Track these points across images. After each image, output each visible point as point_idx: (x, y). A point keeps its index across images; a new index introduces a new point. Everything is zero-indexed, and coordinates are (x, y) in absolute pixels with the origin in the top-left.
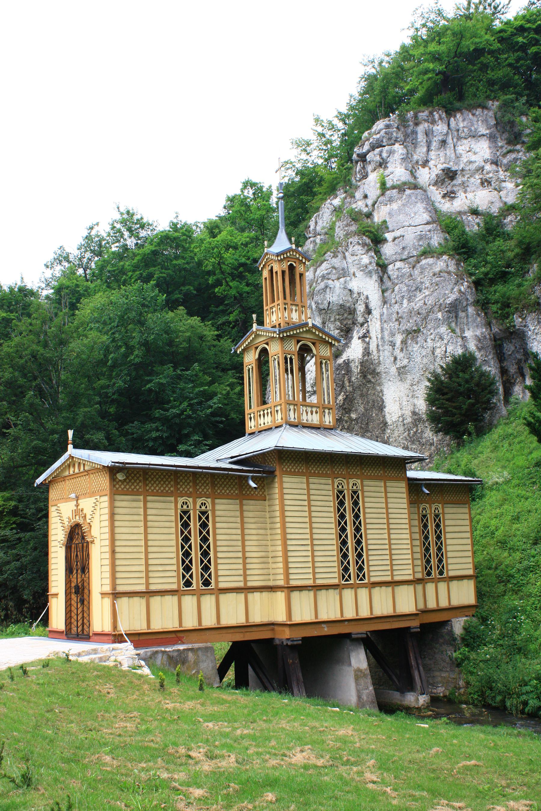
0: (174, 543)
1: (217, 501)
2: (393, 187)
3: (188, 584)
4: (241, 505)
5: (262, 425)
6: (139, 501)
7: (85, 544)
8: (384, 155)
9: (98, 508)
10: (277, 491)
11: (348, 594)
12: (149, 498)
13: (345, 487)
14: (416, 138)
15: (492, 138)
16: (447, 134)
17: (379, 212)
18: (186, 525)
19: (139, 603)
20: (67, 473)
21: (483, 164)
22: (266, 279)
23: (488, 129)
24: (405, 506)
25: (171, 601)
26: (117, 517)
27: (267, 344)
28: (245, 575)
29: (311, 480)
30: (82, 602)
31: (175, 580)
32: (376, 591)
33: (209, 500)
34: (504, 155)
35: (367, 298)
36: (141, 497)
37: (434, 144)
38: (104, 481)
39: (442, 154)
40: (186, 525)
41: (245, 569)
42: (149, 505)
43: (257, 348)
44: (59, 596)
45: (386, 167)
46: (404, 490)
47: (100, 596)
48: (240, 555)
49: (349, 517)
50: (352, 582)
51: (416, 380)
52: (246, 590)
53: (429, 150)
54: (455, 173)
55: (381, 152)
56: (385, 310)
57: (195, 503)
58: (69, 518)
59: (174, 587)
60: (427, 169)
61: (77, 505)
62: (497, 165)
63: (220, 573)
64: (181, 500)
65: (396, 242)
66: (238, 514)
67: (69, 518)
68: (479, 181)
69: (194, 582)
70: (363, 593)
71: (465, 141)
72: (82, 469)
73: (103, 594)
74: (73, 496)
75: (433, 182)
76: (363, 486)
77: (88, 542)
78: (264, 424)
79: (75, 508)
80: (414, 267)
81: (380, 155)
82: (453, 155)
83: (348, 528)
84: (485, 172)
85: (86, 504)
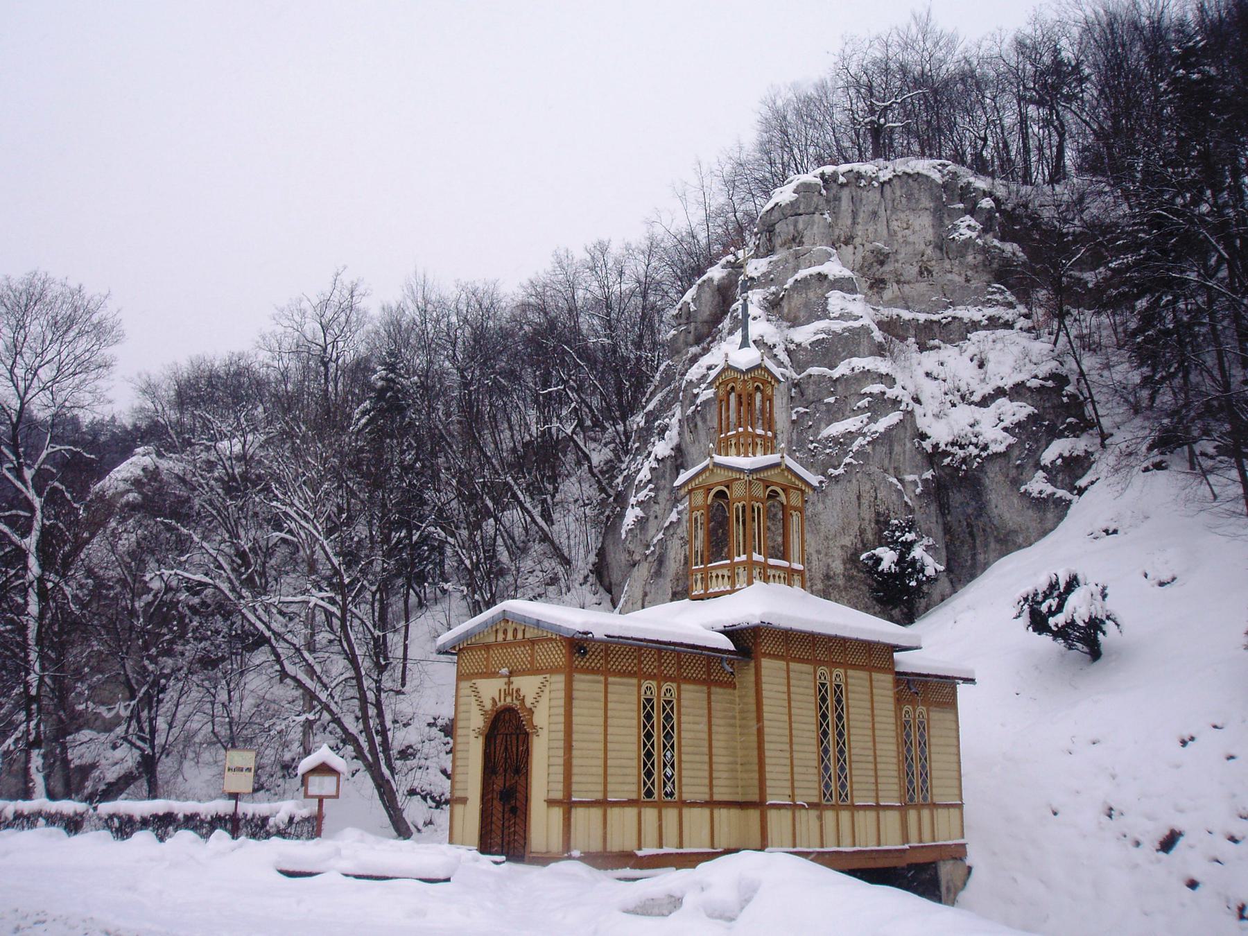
0: (635, 739)
1: (683, 686)
3: (649, 793)
4: (709, 694)
6: (599, 682)
7: (521, 737)
8: (801, 226)
9: (547, 690)
10: (753, 678)
11: (829, 816)
12: (611, 679)
13: (828, 678)
14: (839, 206)
16: (879, 204)
17: (789, 303)
18: (649, 717)
19: (596, 813)
21: (923, 246)
23: (932, 200)
24: (892, 707)
25: (631, 812)
26: (575, 703)
27: (727, 487)
28: (711, 786)
29: (793, 665)
30: (514, 810)
31: (635, 788)
32: (860, 815)
33: (675, 685)
36: (602, 678)
37: (862, 215)
38: (558, 656)
39: (871, 229)
40: (649, 717)
41: (711, 778)
42: (610, 688)
43: (709, 490)
45: (801, 243)
46: (891, 685)
48: (706, 758)
49: (831, 717)
50: (833, 802)
51: (833, 532)
52: (711, 804)
53: (854, 223)
54: (887, 255)
55: (796, 223)
56: (795, 437)
57: (659, 688)
58: (493, 699)
59: (634, 796)
60: (851, 247)
61: (509, 683)
62: (941, 249)
63: (684, 781)
64: (645, 684)
66: (705, 703)
67: (493, 699)
68: (917, 269)
69: (656, 792)
70: (845, 816)
71: (902, 216)
72: (520, 636)
73: (551, 803)
74: (505, 671)
75: (857, 267)
76: (846, 676)
77: (527, 734)
81: (795, 226)
82: (885, 232)
83: (830, 732)
84: (925, 258)
85: (527, 685)
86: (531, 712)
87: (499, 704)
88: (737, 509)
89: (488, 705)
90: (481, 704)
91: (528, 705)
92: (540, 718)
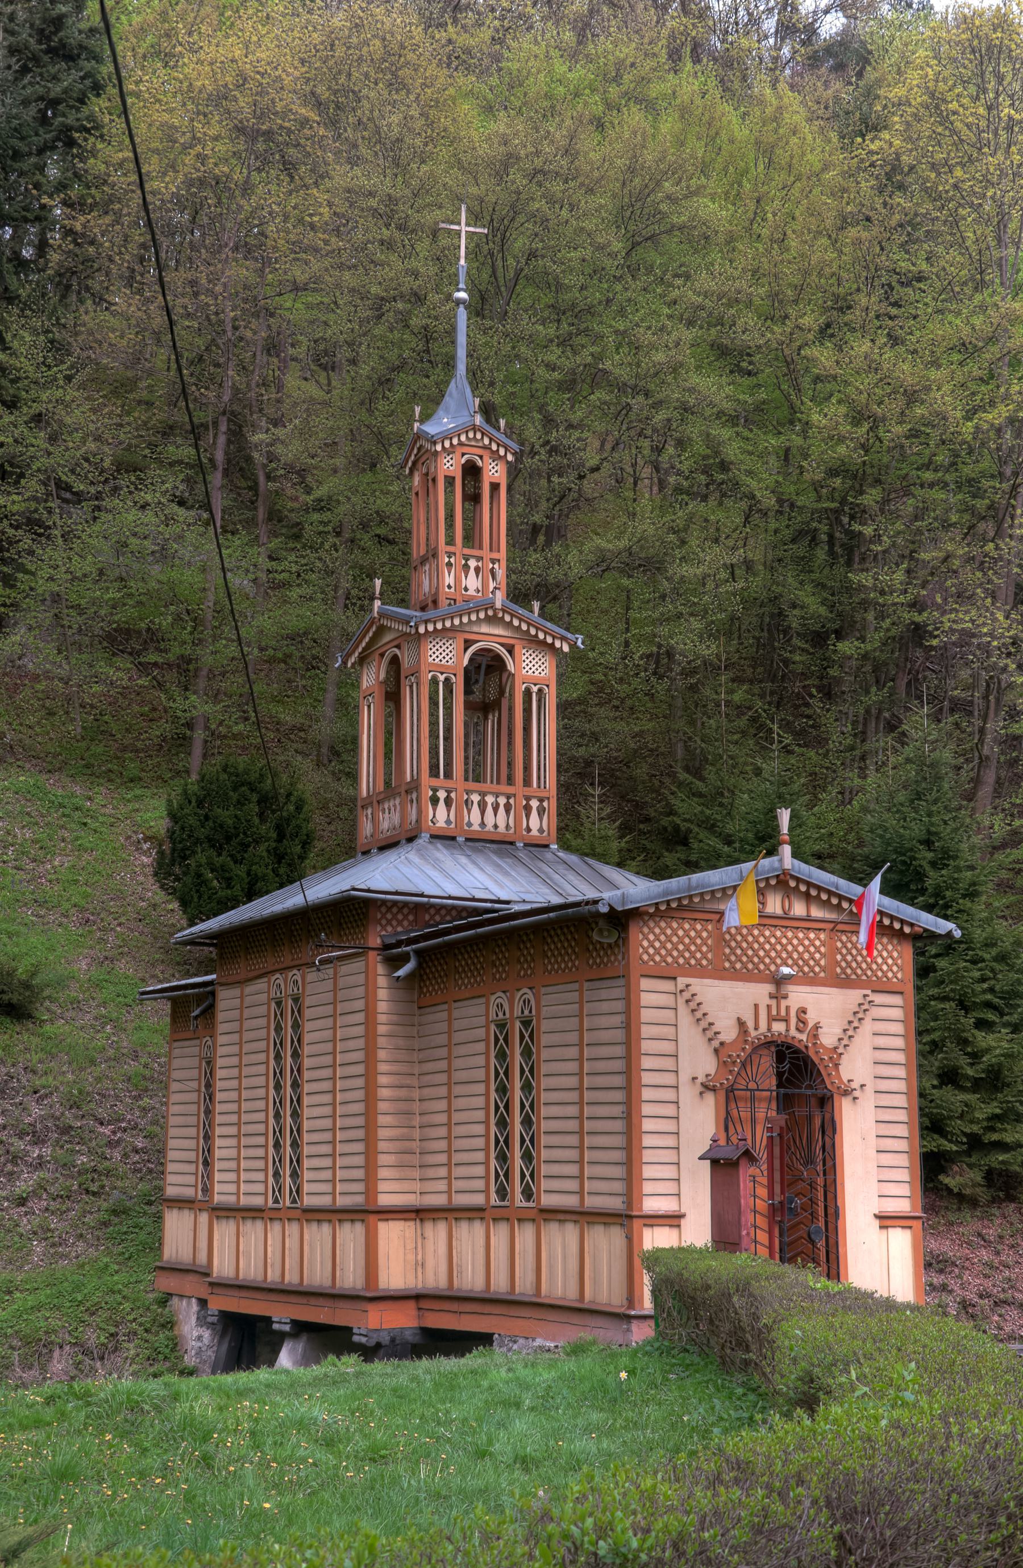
5: (476, 827)
22: (450, 481)
27: (510, 650)
43: (468, 644)
44: (683, 1222)
47: (876, 1223)
58: (741, 1023)
61: (778, 996)
67: (741, 1023)
73: (886, 1221)
78: (483, 824)
79: (773, 1003)
86: (836, 1055)
87: (753, 1034)
88: (528, 693)
89: (729, 1034)
90: (709, 1030)
91: (828, 1038)
92: (856, 1067)
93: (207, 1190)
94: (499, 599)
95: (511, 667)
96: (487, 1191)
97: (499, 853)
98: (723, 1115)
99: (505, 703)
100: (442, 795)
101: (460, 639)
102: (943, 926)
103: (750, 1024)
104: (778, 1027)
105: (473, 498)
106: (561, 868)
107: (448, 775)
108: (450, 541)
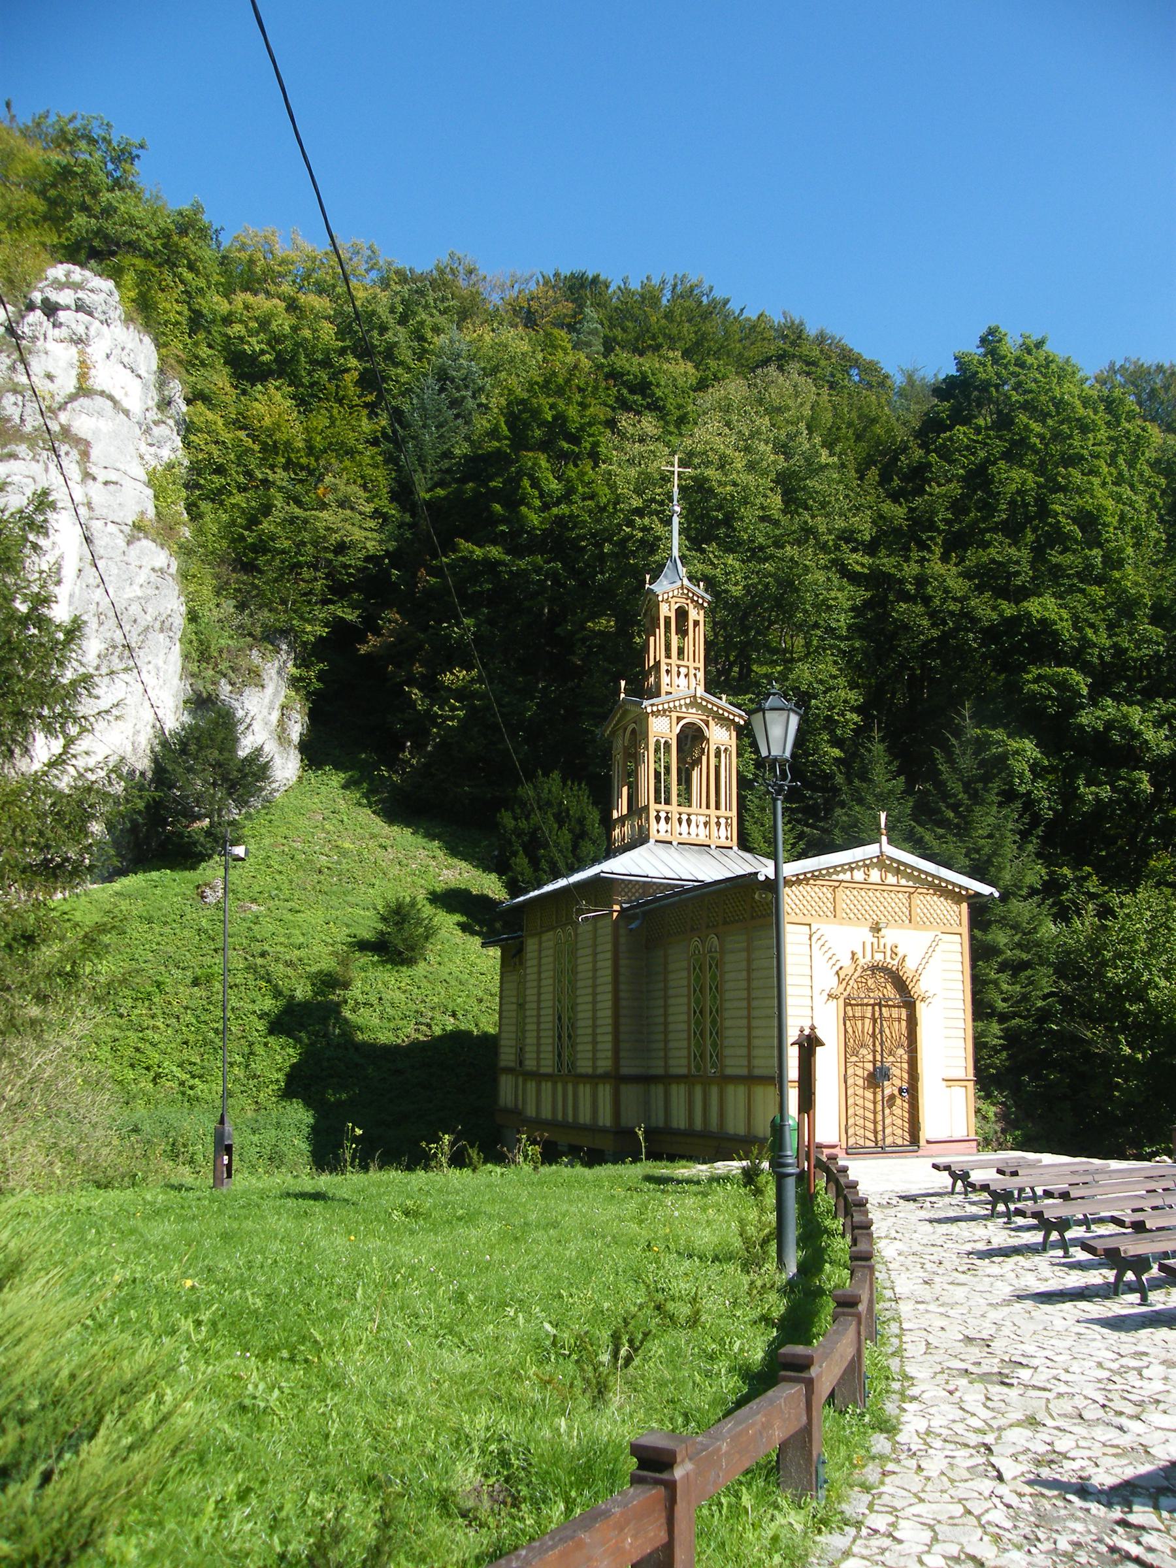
2: (102, 393)
8: (92, 332)
15: (145, 386)
20: (847, 876)
34: (156, 423)
35: (62, 557)
43: (679, 719)
65: (112, 487)
80: (129, 543)
91: (910, 966)
93: (521, 1063)
94: (700, 691)
95: (707, 733)
96: (689, 1066)
97: (699, 852)
98: (842, 1014)
99: (704, 758)
100: (663, 815)
101: (674, 715)
102: (986, 890)
103: (859, 955)
104: (879, 957)
105: (682, 632)
106: (740, 861)
107: (668, 802)
108: (668, 656)
